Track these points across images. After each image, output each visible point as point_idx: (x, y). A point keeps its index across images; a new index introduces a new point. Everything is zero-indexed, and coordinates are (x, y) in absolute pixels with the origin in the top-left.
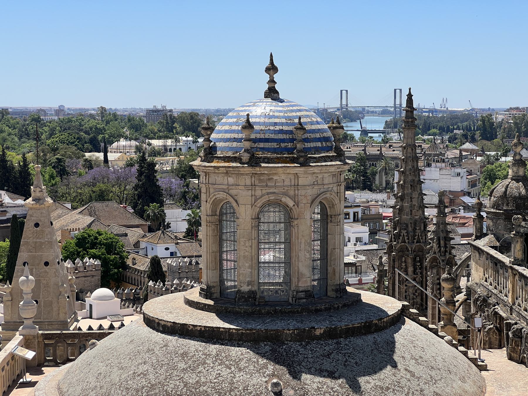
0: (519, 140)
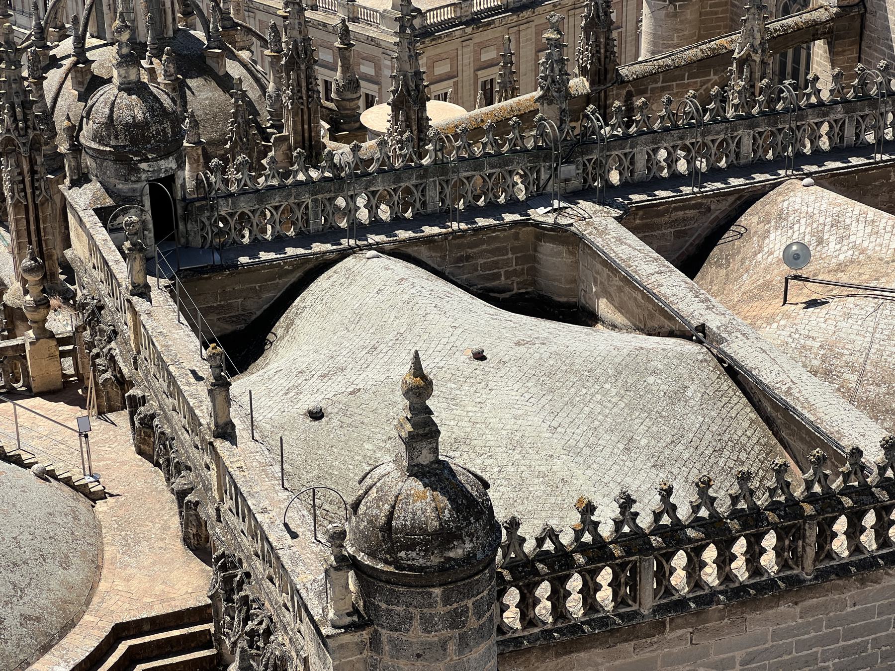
0: (123, 21)
